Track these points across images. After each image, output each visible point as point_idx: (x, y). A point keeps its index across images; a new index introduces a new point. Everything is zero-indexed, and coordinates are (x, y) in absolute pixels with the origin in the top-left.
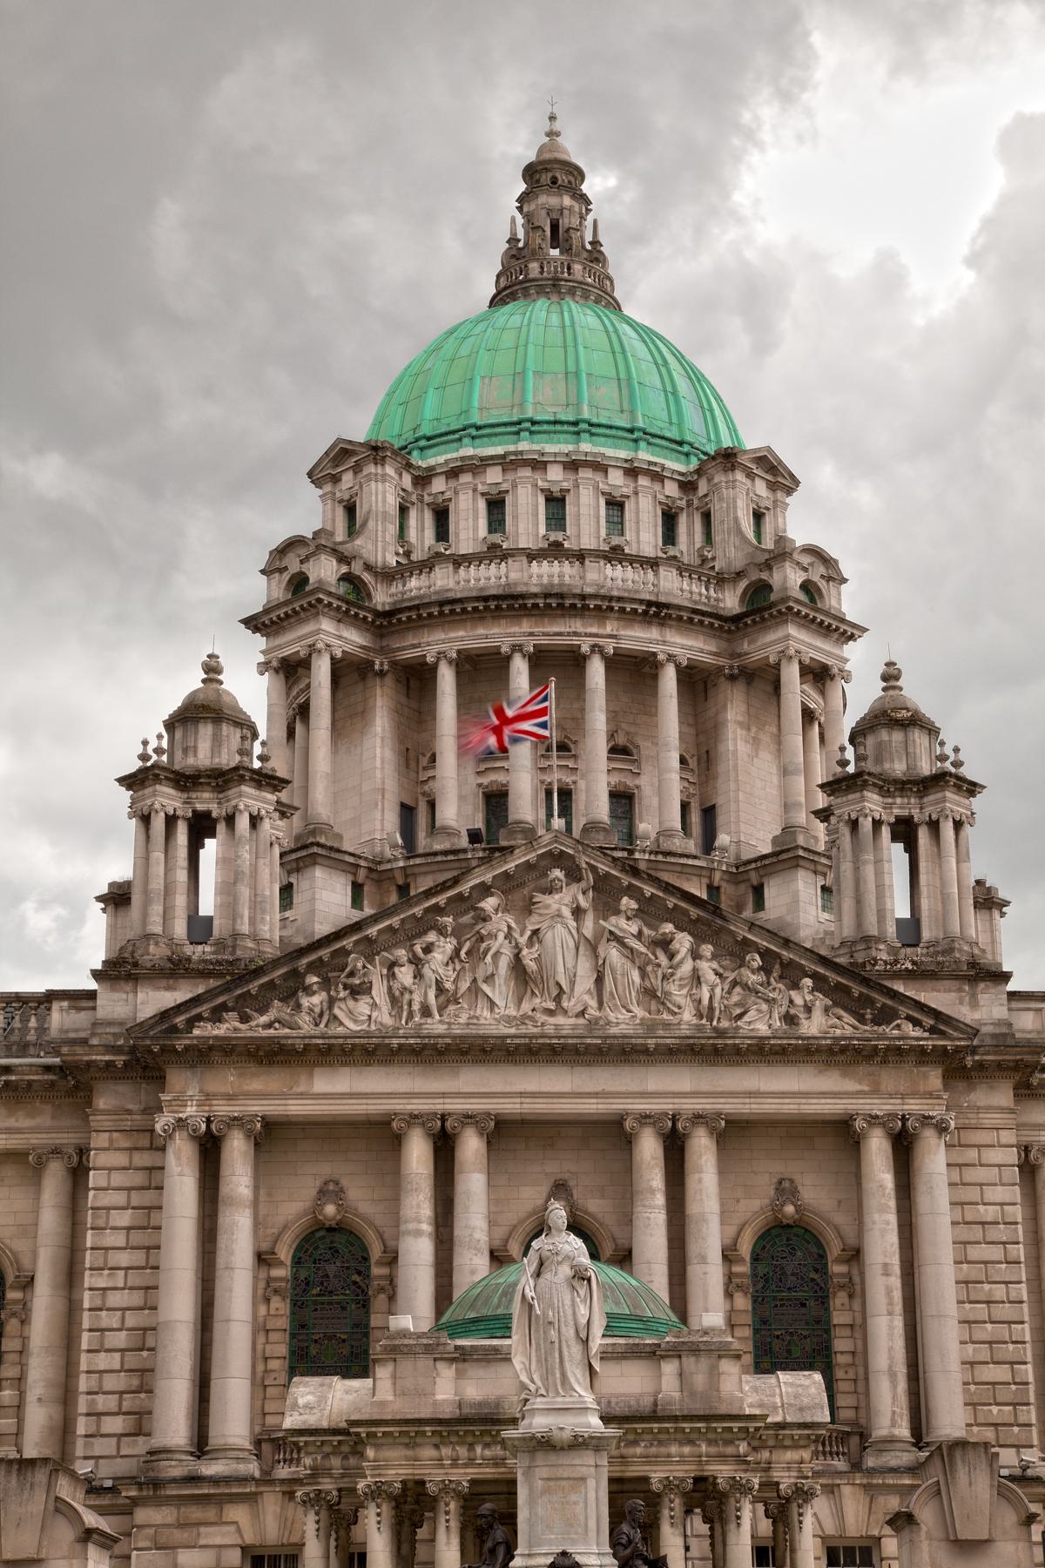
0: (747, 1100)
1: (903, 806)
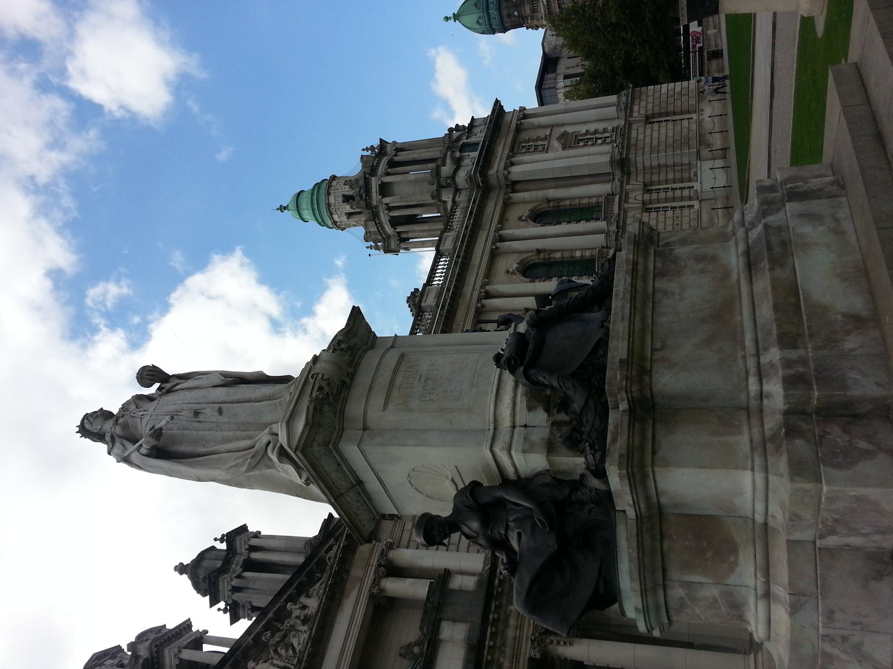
0: (344, 657)
1: (236, 568)
